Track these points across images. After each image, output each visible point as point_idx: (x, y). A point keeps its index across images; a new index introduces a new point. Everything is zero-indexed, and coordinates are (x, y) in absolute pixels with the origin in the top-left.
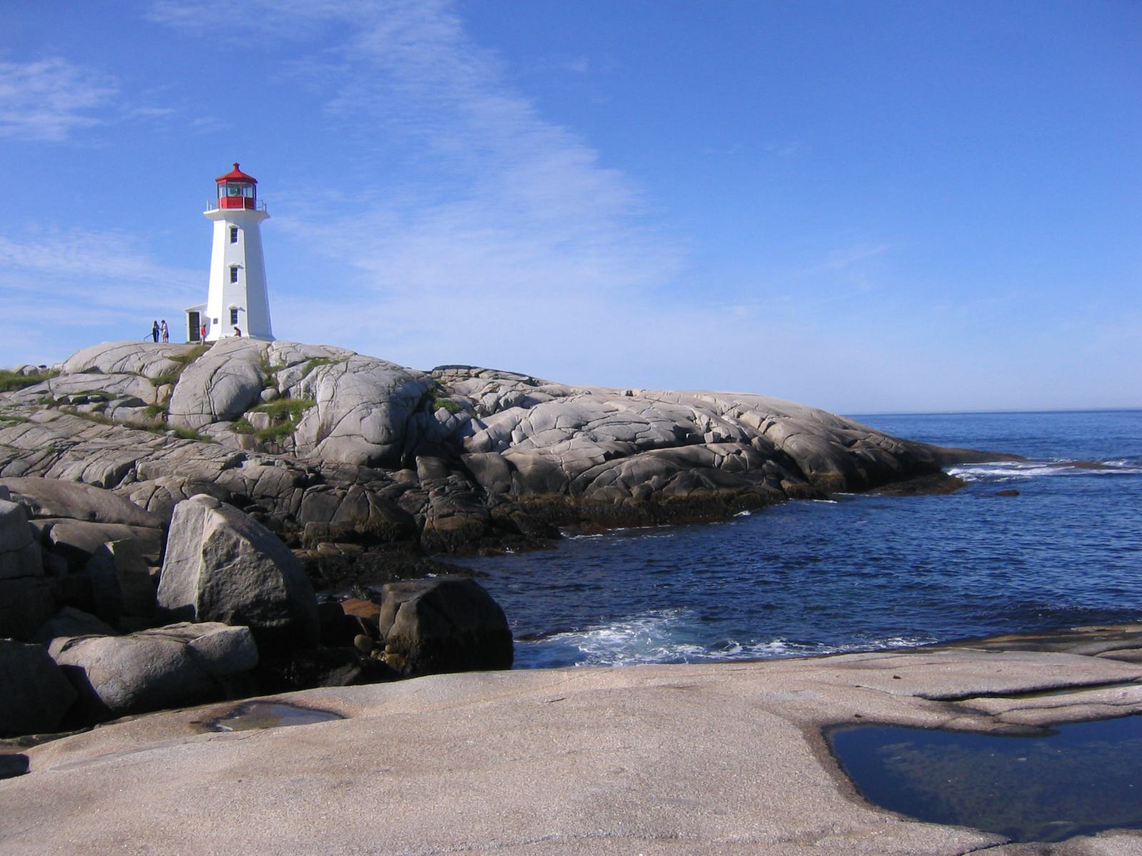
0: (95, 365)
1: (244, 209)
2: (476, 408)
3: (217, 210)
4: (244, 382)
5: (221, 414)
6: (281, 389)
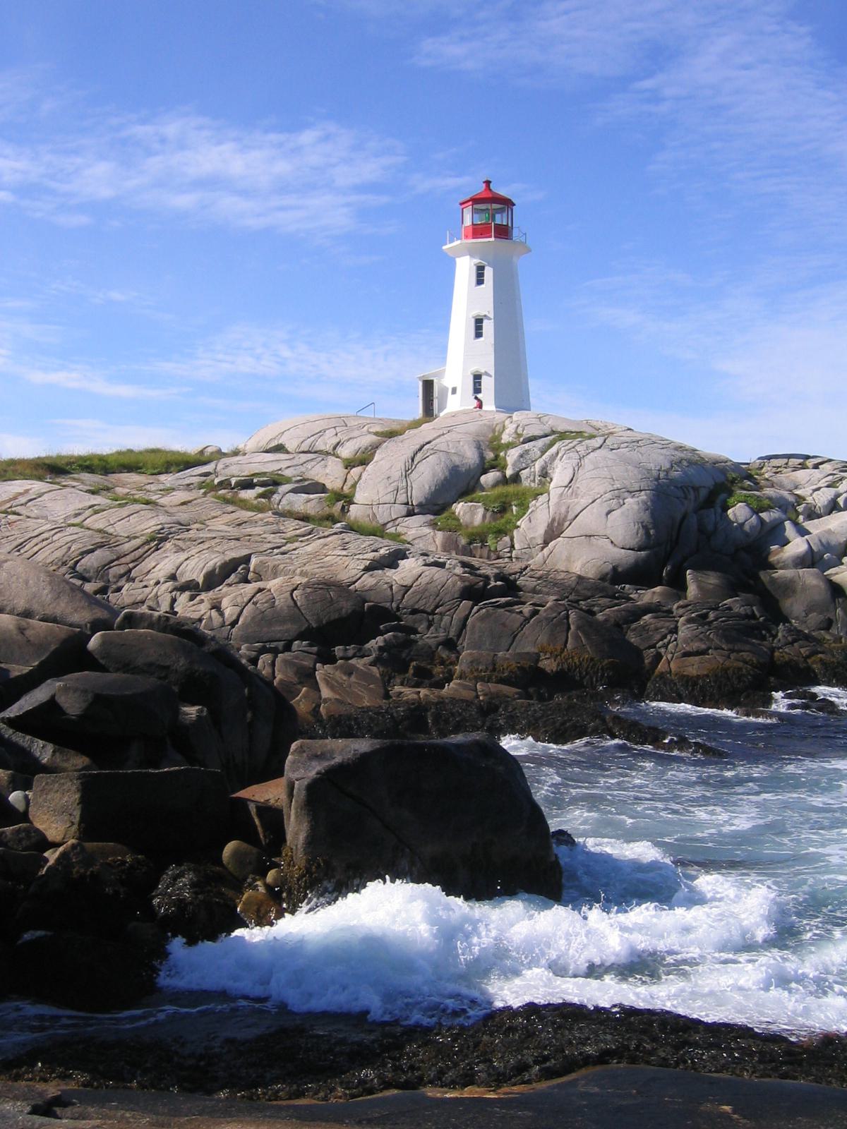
0: (280, 442)
1: (492, 239)
2: (800, 509)
3: (459, 242)
4: (457, 460)
5: (420, 505)
6: (509, 472)
